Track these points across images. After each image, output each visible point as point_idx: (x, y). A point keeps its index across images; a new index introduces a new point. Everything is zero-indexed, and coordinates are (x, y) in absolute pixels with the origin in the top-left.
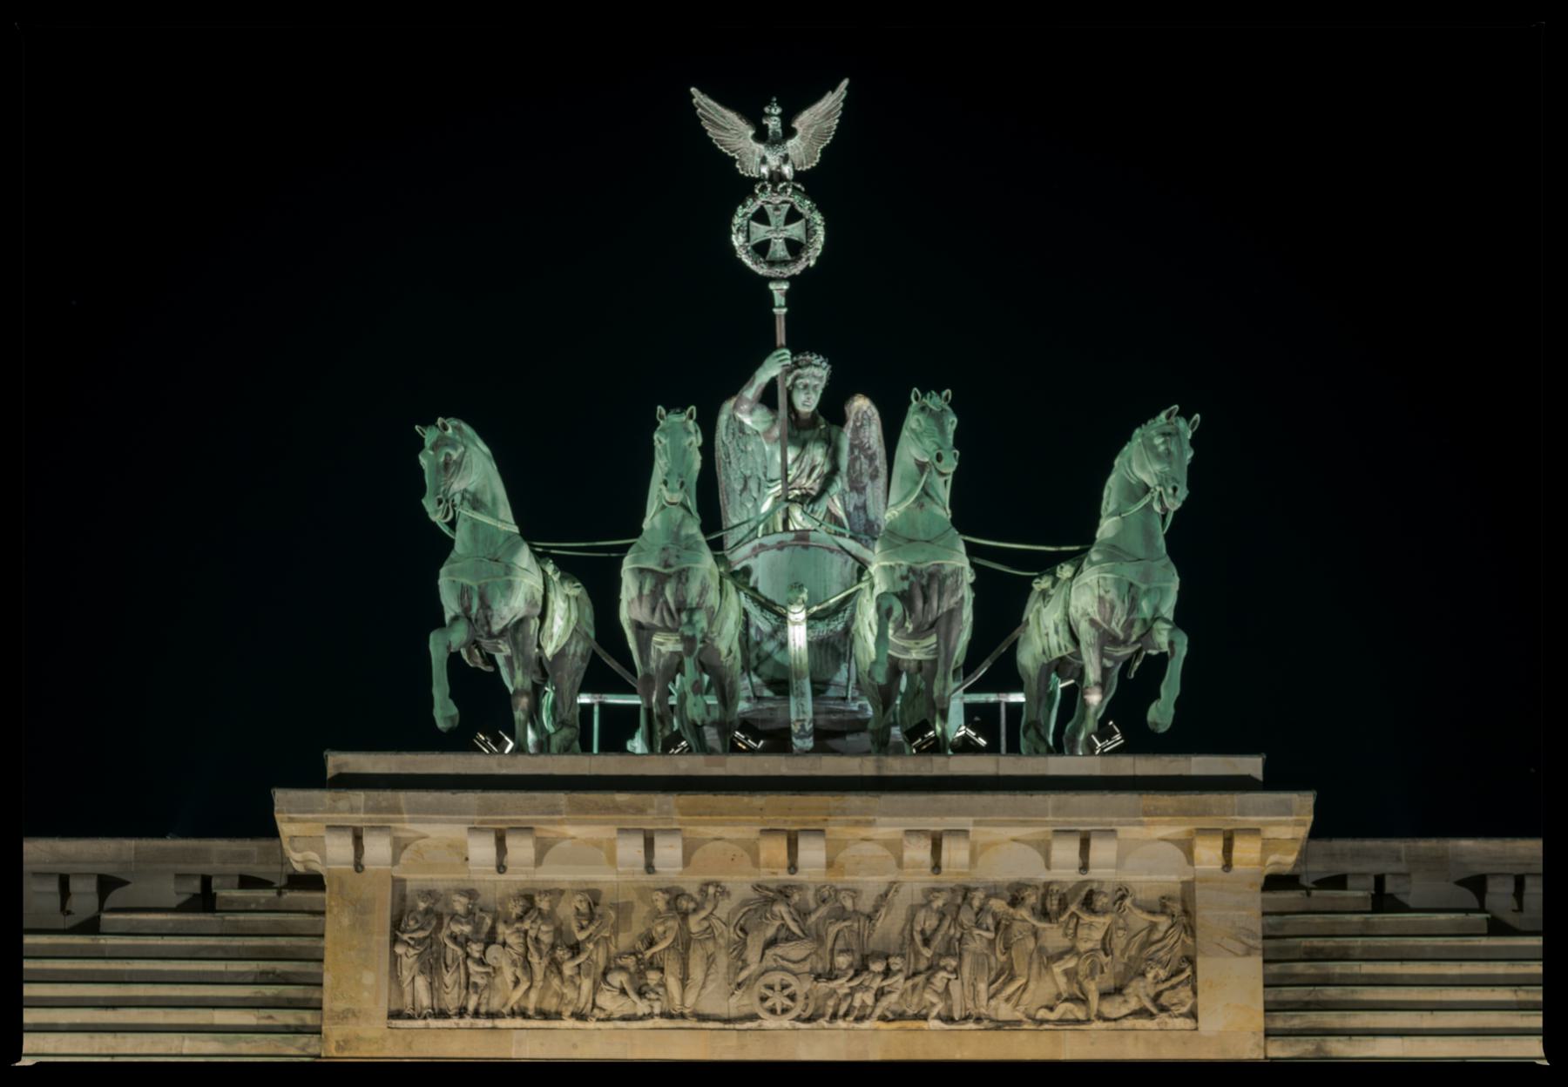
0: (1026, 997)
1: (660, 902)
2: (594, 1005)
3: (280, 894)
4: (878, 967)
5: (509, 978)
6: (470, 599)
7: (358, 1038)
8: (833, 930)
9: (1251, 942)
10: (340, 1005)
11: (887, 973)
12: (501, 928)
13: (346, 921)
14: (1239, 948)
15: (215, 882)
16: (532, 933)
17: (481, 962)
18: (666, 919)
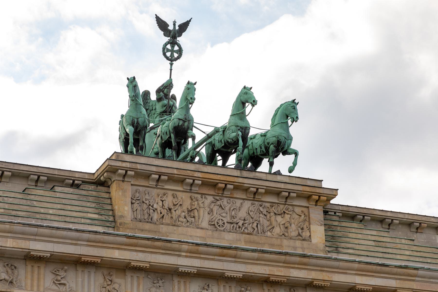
0: (274, 230)
1: (193, 198)
2: (179, 221)
3: (97, 186)
4: (243, 219)
5: (159, 212)
6: (135, 121)
7: (124, 223)
8: (232, 209)
9: (322, 223)
10: (120, 214)
11: (244, 220)
12: (157, 200)
13: (120, 194)
14: (319, 224)
15: (76, 182)
16: (164, 202)
17: (152, 206)
18: (194, 202)
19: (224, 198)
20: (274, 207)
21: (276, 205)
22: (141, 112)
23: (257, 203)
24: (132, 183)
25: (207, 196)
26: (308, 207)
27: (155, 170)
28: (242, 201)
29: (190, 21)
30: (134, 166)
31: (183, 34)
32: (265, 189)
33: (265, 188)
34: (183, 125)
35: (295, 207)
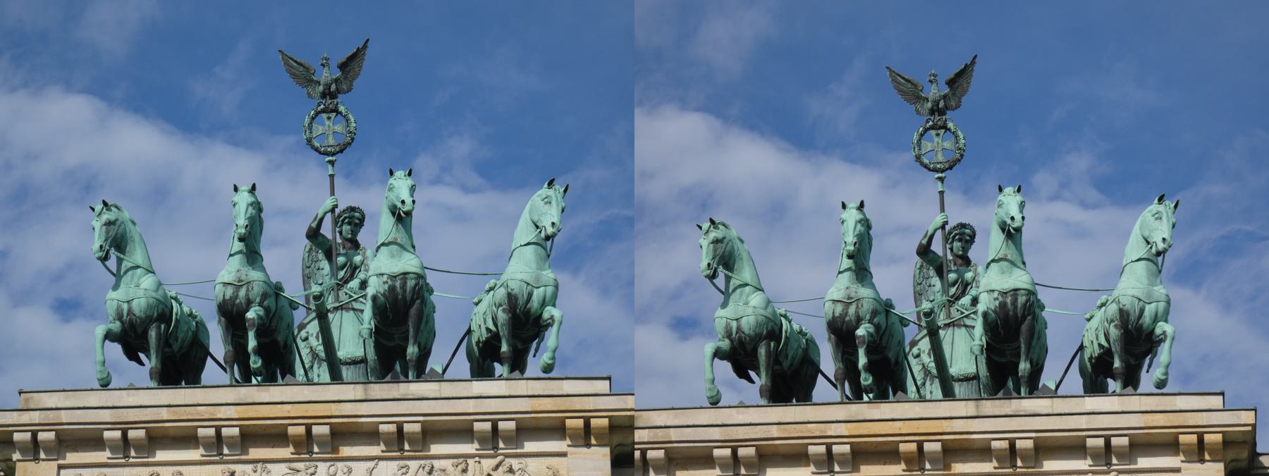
19: (319, 464)
20: (460, 468)
21: (469, 461)
22: (138, 286)
23: (414, 465)
24: (61, 462)
25: (269, 466)
26: (564, 455)
27: (108, 420)
28: (371, 464)
29: (365, 46)
30: (51, 417)
31: (356, 83)
32: (422, 423)
33: (421, 418)
34: (235, 296)
35: (529, 460)
